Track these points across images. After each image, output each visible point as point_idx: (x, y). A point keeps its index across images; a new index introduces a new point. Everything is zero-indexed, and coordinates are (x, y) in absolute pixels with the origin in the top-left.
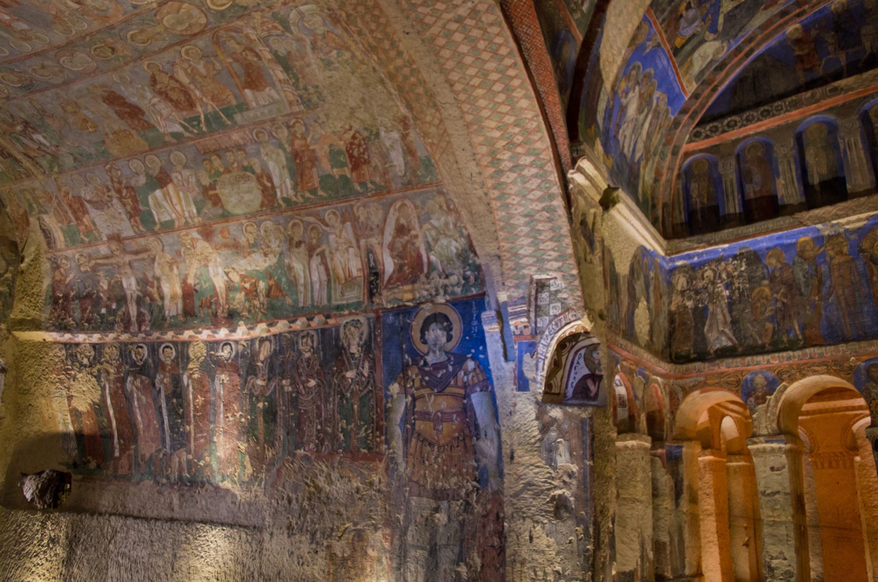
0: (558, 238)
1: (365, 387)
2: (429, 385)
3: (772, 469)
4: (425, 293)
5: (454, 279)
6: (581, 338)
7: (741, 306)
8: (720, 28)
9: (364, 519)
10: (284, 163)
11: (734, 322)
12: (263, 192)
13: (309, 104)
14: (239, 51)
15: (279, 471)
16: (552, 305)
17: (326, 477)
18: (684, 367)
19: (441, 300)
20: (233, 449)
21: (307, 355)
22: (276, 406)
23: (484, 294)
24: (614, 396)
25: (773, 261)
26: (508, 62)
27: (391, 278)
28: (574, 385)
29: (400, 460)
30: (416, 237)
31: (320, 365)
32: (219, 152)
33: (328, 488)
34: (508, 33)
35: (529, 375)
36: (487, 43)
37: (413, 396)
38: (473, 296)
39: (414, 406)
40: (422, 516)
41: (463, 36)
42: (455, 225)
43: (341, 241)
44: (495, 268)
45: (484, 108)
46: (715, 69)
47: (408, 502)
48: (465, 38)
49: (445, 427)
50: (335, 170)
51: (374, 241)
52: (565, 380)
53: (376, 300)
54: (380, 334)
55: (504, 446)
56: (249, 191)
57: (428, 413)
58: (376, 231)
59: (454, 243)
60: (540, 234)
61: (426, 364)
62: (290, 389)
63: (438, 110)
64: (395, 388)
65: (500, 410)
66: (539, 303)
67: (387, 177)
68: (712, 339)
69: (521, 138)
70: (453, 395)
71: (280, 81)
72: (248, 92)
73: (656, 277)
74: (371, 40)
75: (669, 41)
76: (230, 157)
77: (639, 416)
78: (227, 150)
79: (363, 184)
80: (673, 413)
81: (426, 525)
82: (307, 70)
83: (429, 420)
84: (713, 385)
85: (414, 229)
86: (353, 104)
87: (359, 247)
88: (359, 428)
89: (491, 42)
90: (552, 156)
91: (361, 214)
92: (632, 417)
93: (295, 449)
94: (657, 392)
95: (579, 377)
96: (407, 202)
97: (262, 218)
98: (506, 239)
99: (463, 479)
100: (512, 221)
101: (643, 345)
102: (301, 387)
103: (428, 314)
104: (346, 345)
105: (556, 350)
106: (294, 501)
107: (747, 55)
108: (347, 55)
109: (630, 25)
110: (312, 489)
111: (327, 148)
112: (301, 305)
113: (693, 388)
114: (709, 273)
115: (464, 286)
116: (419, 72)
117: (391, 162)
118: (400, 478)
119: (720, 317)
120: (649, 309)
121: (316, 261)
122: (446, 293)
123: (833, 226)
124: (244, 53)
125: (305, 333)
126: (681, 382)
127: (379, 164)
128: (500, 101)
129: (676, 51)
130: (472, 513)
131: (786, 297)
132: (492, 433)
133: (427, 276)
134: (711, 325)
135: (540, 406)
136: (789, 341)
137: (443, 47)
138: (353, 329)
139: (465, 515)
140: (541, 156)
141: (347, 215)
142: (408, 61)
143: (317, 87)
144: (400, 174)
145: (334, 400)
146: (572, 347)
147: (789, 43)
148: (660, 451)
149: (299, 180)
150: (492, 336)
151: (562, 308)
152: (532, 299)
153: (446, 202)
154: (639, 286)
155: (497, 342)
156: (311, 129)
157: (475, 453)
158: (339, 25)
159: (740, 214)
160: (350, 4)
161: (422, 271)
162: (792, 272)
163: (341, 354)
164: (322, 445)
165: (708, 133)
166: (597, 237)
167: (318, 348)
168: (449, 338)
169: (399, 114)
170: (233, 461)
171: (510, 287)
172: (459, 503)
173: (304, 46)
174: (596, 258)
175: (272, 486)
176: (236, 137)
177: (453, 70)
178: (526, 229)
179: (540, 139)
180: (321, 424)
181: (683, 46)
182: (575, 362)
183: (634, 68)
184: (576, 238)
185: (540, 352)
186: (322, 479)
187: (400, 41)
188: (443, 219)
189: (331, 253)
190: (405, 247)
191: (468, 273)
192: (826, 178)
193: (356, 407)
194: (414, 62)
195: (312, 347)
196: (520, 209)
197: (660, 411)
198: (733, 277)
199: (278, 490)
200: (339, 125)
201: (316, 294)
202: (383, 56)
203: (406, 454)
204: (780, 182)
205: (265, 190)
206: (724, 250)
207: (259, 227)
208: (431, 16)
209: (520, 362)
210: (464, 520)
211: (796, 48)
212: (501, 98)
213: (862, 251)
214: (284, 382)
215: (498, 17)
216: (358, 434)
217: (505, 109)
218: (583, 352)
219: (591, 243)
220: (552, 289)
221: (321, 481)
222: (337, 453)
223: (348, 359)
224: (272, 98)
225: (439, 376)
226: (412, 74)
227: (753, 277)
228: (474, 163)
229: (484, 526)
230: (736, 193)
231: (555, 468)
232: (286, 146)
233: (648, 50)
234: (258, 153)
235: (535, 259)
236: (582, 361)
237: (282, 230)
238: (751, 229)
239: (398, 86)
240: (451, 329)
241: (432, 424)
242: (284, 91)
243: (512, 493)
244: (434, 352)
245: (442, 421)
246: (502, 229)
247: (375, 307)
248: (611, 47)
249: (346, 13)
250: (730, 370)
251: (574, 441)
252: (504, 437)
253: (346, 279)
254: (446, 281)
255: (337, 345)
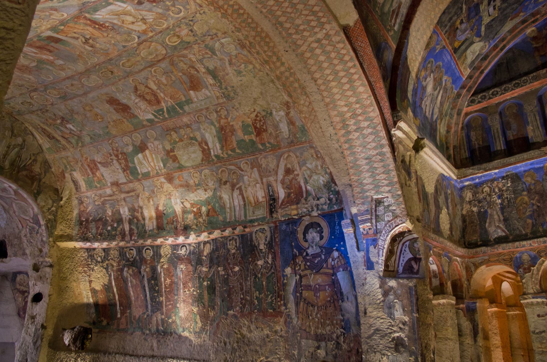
0: (387, 172)
1: (270, 270)
2: (311, 268)
3: (539, 316)
4: (305, 210)
5: (322, 200)
6: (406, 234)
7: (510, 209)
8: (483, 34)
9: (272, 354)
10: (215, 133)
11: (506, 220)
12: (203, 152)
13: (228, 98)
14: (186, 68)
15: (218, 324)
16: (386, 215)
17: (247, 328)
18: (474, 250)
19: (315, 214)
20: (189, 311)
21: (233, 251)
22: (215, 284)
23: (342, 209)
24: (430, 271)
25: (529, 179)
26: (350, 64)
27: (283, 201)
28: (403, 265)
29: (294, 316)
30: (298, 175)
31: (242, 257)
32: (175, 129)
33: (249, 335)
34: (349, 47)
35: (374, 259)
36: (336, 54)
37: (300, 275)
38: (336, 210)
39: (301, 282)
40: (309, 352)
41: (321, 51)
42: (322, 167)
43: (251, 180)
44: (348, 192)
45: (337, 94)
46: (482, 60)
47: (300, 343)
48: (323, 52)
49: (321, 294)
50: (246, 137)
51: (271, 179)
52: (397, 262)
53: (274, 215)
54: (278, 236)
55: (360, 306)
56: (194, 152)
57: (310, 286)
58: (273, 173)
59: (321, 178)
60: (376, 170)
61: (307, 254)
62: (223, 273)
63: (308, 97)
64: (288, 270)
65: (356, 283)
66: (378, 213)
67: (278, 139)
68: (491, 231)
69: (360, 111)
70: (326, 274)
71: (211, 85)
72: (192, 92)
73: (452, 193)
74: (265, 57)
75: (451, 44)
76: (182, 132)
77: (447, 284)
78: (180, 128)
79: (263, 144)
80: (469, 281)
81: (312, 358)
82: (227, 77)
83: (311, 290)
84: (494, 261)
85: (296, 170)
86: (255, 95)
87: (262, 183)
88: (267, 296)
89: (339, 53)
90: (381, 120)
91: (263, 162)
92: (442, 284)
93: (228, 311)
94: (457, 267)
95: (406, 259)
96: (291, 154)
97: (203, 168)
98: (354, 174)
99: (334, 327)
100: (358, 163)
101: (446, 237)
102: (230, 271)
103: (307, 223)
104: (257, 244)
105: (391, 243)
106: (228, 344)
107: (502, 49)
108: (251, 67)
109: (425, 36)
110: (239, 336)
111: (240, 124)
112: (228, 220)
113: (481, 264)
114: (487, 189)
115: (329, 204)
116: (295, 74)
117: (280, 130)
118: (294, 328)
119: (496, 217)
120: (449, 214)
121: (236, 193)
122: (318, 209)
124: (189, 70)
125: (231, 238)
126: (473, 260)
127: (273, 131)
128: (346, 89)
129: (456, 50)
130: (341, 349)
131: (539, 203)
132: (352, 298)
133: (306, 200)
134: (490, 223)
135: (382, 279)
136: (544, 231)
137: (309, 58)
138: (260, 234)
139: (336, 350)
140: (374, 121)
141: (254, 164)
142: (288, 68)
143: (233, 87)
144: (286, 137)
145: (251, 279)
146: (401, 241)
147: (529, 40)
148: (461, 306)
149: (224, 143)
150: (349, 235)
151: (393, 216)
152: (373, 211)
153: (316, 153)
154: (441, 199)
155: (352, 239)
156: (230, 112)
157: (341, 310)
158: (245, 49)
159: (504, 150)
160: (251, 36)
161: (302, 197)
162: (542, 186)
163: (254, 250)
164: (244, 308)
165: (480, 100)
166: (412, 170)
167: (240, 247)
168: (321, 238)
169: (284, 101)
170: (189, 319)
171: (359, 204)
172: (332, 343)
173: (225, 64)
174: (413, 183)
175: (214, 334)
176: (185, 120)
177: (316, 72)
178: (367, 167)
179: (373, 110)
180: (243, 294)
181: (460, 47)
182: (403, 250)
183: (429, 63)
184: (399, 171)
185: (380, 244)
186: (245, 329)
187: (282, 56)
188: (314, 163)
189: (245, 187)
190: (291, 181)
191: (332, 196)
193: (264, 283)
194: (291, 68)
195: (236, 246)
196: (363, 155)
197: (460, 280)
198: (503, 191)
199: (218, 337)
200: (247, 109)
201: (237, 213)
202: (272, 66)
203: (297, 312)
204: (530, 128)
205: (203, 151)
206: (495, 173)
207: (201, 173)
208: (301, 40)
209: (368, 251)
210: (336, 354)
211: (534, 43)
212: (347, 87)
214: (219, 269)
215: (342, 37)
216: (267, 300)
217: (349, 93)
218: (407, 243)
219: (409, 174)
220: (386, 204)
221: (245, 331)
222: (254, 312)
223: (258, 253)
224: (206, 95)
225: (316, 262)
226: (291, 76)
227: (516, 190)
228: (332, 128)
229: (349, 358)
230: (501, 137)
231: (394, 319)
232: (216, 123)
233: (437, 51)
234: (199, 129)
235: (373, 186)
236: (407, 249)
237: (215, 174)
238: (512, 159)
239: (283, 83)
240: (322, 232)
241: (313, 293)
242: (213, 91)
243: (366, 336)
244: (312, 247)
245: (319, 291)
246: (352, 168)
247: (274, 220)
248: (414, 51)
249: (249, 42)
250: (505, 251)
251: (405, 301)
252: (360, 300)
253: (255, 203)
254: (318, 202)
255: (251, 245)
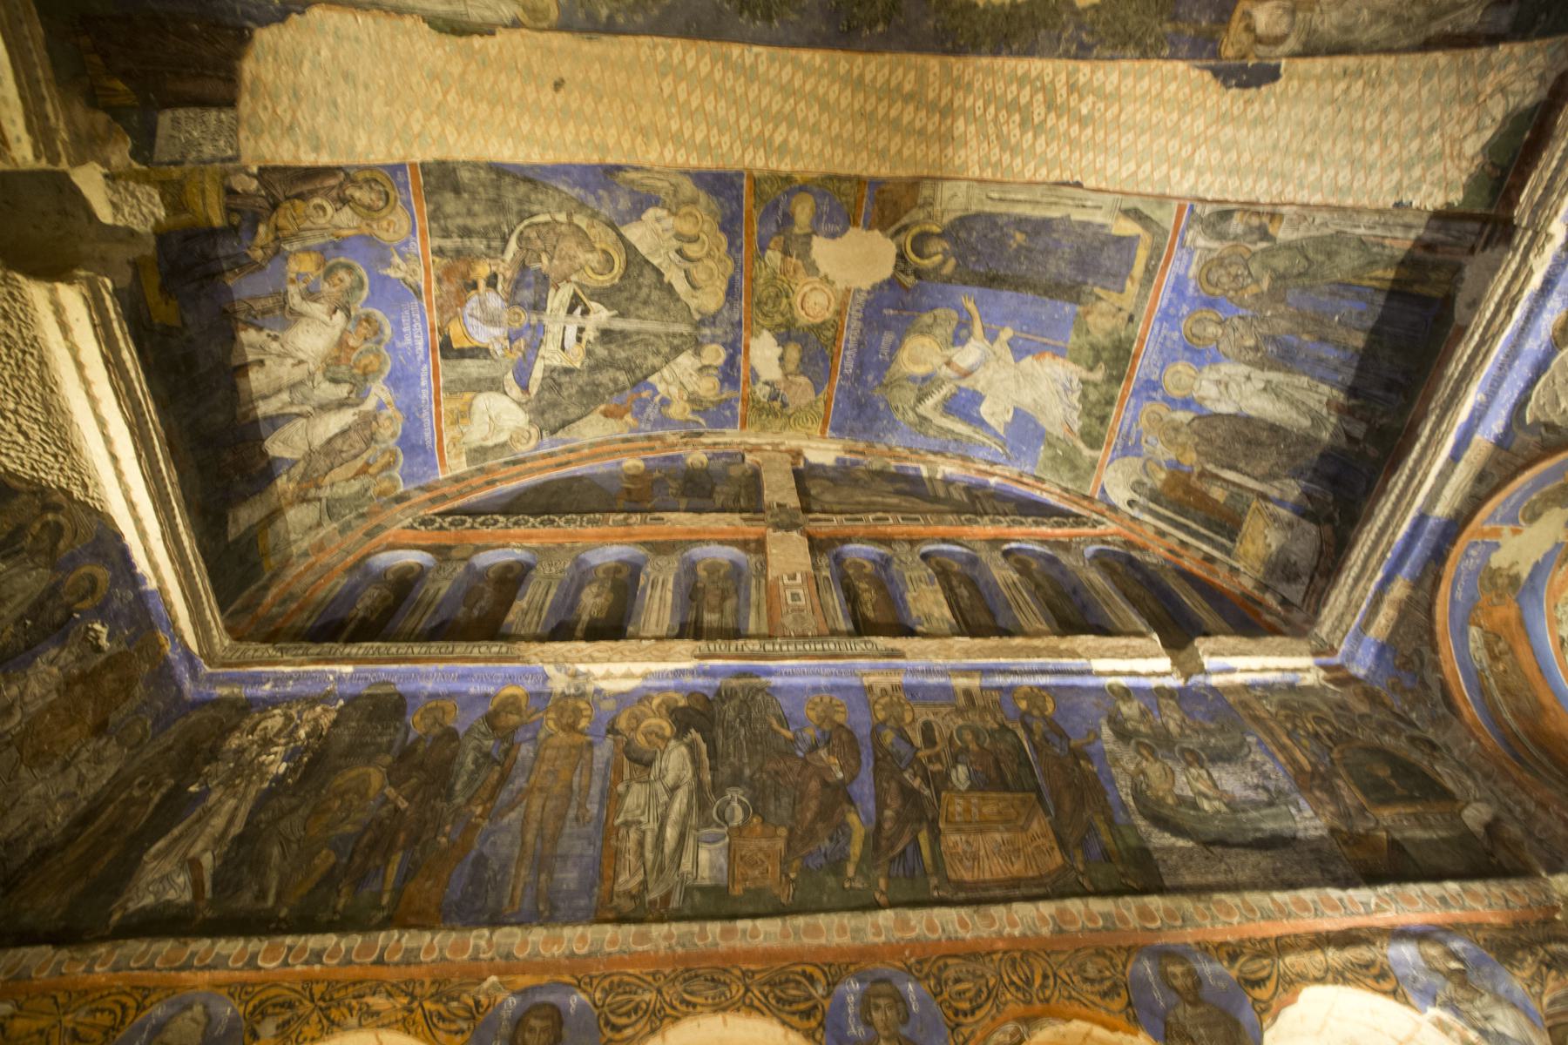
8: (534, 389)
123: (575, 675)
192: (597, 620)
206: (340, 679)
213: (612, 730)
